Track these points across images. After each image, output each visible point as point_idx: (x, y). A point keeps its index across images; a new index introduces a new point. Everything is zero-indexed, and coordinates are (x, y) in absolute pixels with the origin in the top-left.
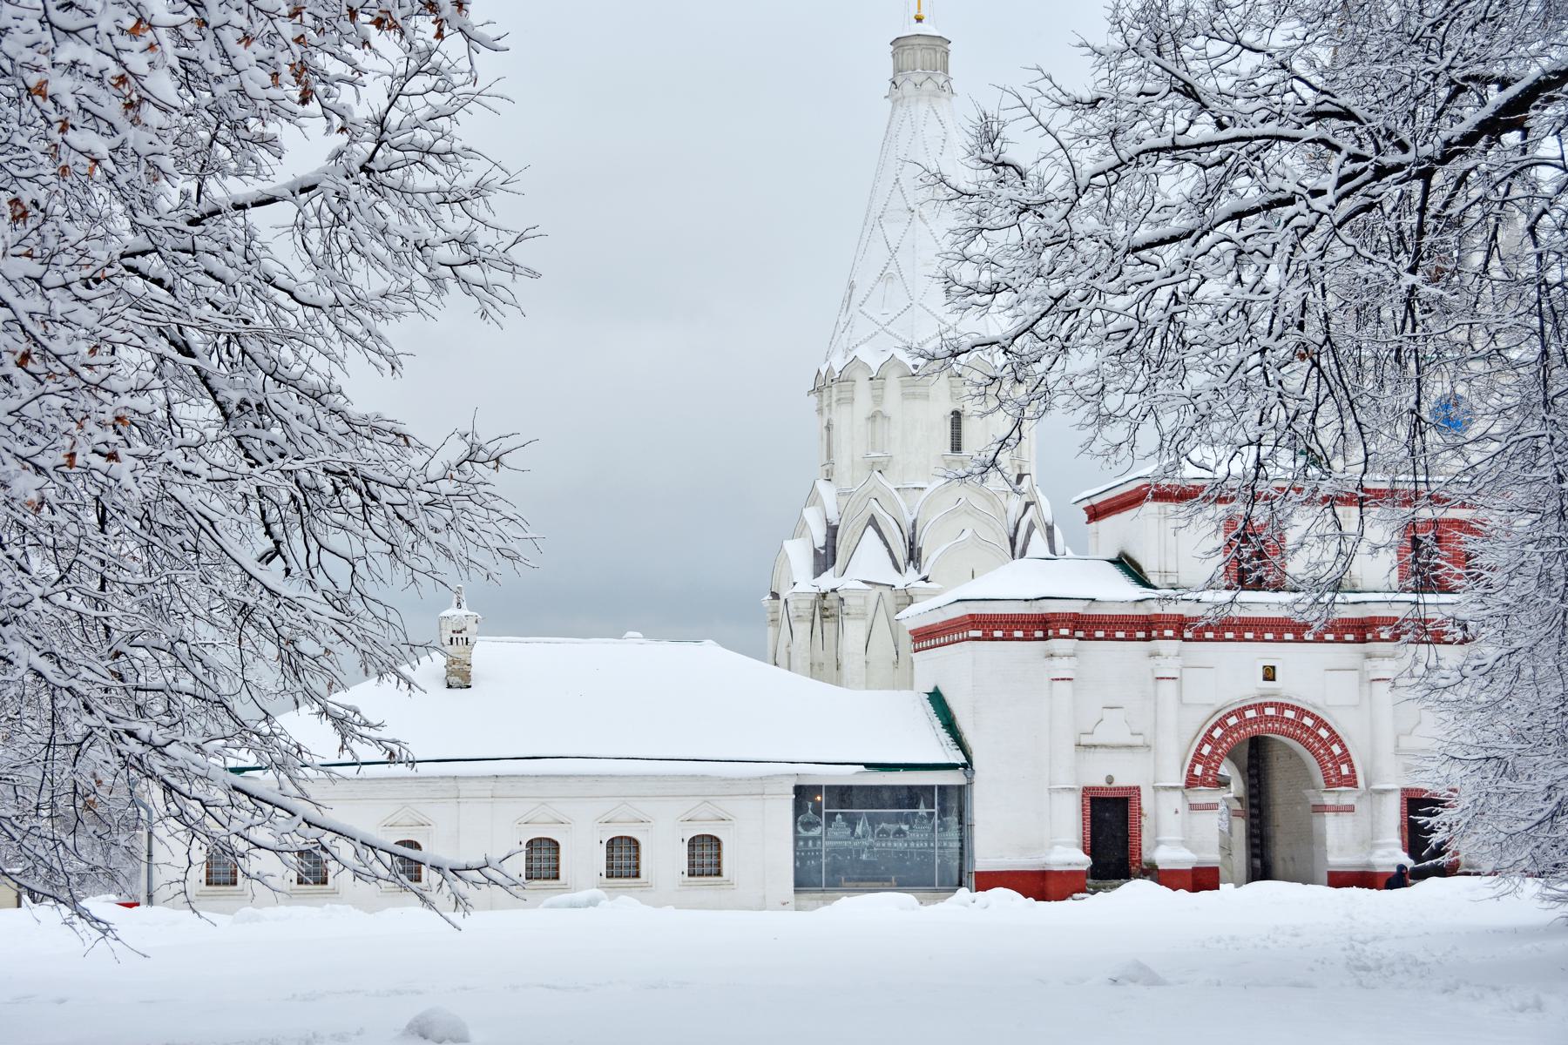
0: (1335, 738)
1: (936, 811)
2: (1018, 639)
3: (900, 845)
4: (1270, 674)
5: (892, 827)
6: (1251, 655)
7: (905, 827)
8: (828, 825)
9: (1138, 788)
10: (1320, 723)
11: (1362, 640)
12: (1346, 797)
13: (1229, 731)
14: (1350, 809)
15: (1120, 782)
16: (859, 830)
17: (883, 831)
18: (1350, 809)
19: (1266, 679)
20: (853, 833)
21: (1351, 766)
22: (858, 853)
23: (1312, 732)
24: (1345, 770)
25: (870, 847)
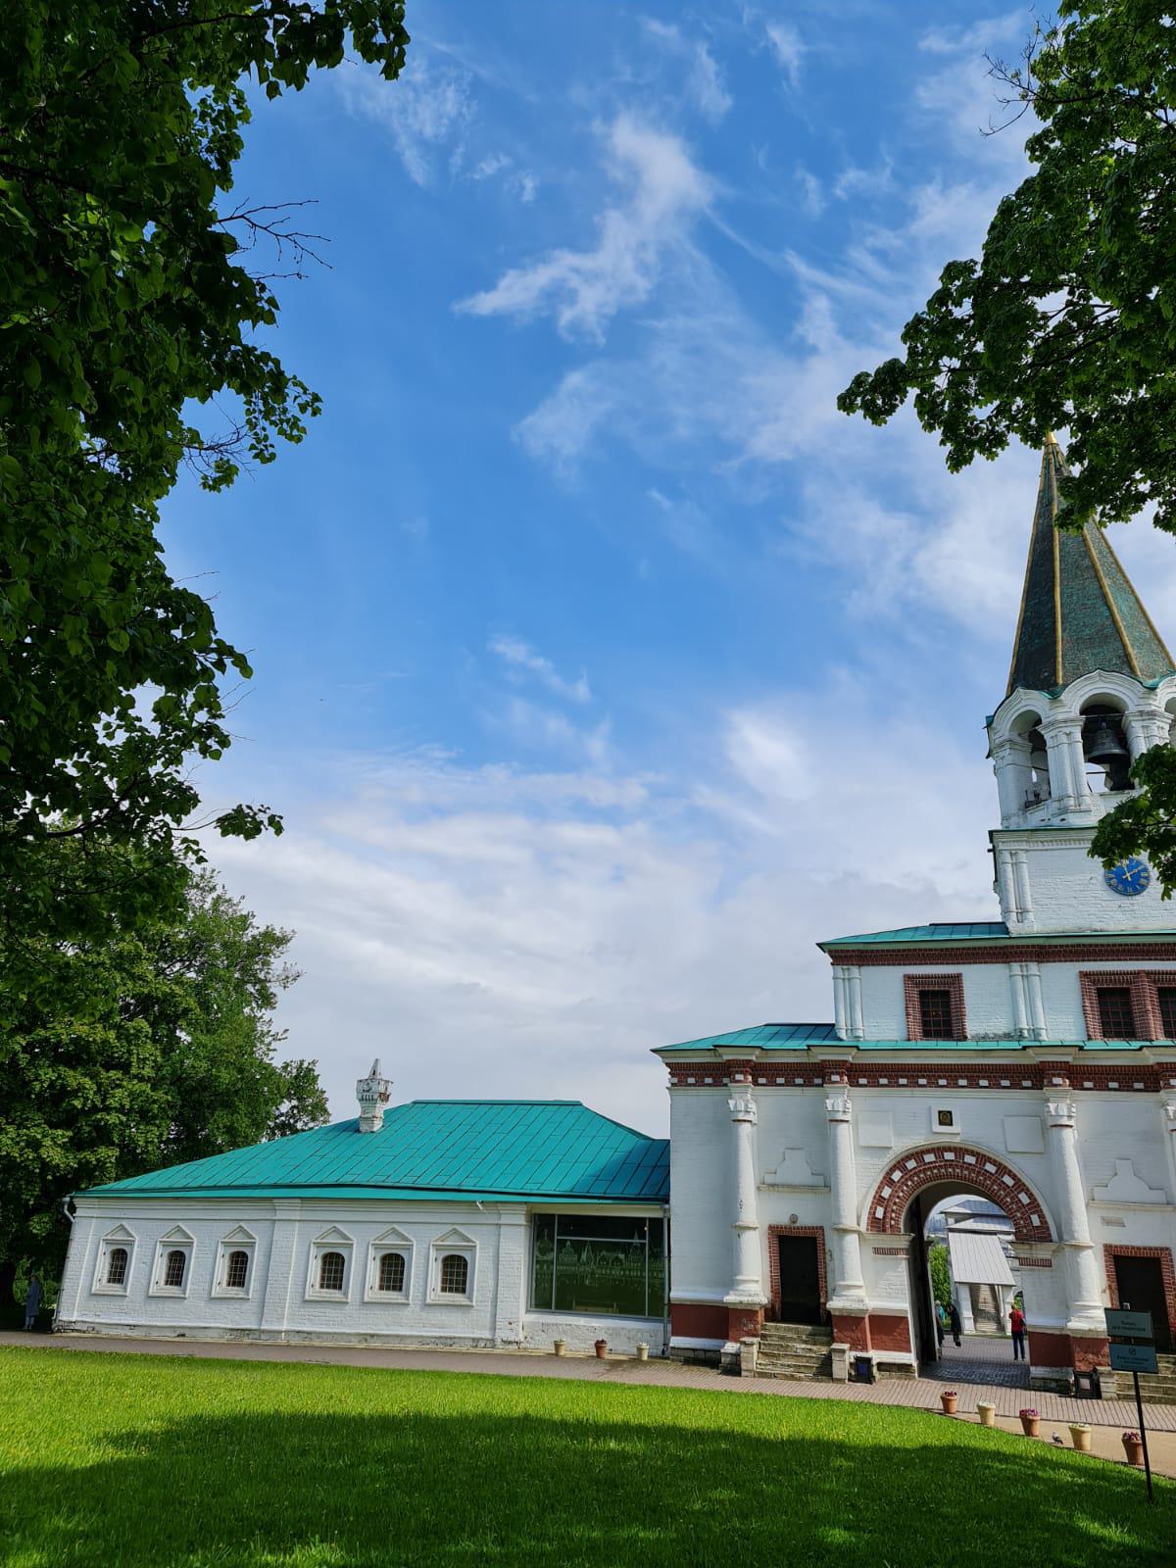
0: (1020, 1186)
2: (709, 1085)
3: (617, 1272)
4: (946, 1118)
7: (622, 1256)
8: (559, 1251)
9: (822, 1228)
10: (1003, 1170)
11: (1038, 1086)
14: (1047, 1264)
15: (807, 1219)
16: (584, 1257)
17: (603, 1258)
18: (1047, 1264)
19: (941, 1123)
20: (579, 1259)
21: (1042, 1217)
22: (583, 1278)
23: (996, 1178)
24: (1036, 1220)
25: (593, 1273)
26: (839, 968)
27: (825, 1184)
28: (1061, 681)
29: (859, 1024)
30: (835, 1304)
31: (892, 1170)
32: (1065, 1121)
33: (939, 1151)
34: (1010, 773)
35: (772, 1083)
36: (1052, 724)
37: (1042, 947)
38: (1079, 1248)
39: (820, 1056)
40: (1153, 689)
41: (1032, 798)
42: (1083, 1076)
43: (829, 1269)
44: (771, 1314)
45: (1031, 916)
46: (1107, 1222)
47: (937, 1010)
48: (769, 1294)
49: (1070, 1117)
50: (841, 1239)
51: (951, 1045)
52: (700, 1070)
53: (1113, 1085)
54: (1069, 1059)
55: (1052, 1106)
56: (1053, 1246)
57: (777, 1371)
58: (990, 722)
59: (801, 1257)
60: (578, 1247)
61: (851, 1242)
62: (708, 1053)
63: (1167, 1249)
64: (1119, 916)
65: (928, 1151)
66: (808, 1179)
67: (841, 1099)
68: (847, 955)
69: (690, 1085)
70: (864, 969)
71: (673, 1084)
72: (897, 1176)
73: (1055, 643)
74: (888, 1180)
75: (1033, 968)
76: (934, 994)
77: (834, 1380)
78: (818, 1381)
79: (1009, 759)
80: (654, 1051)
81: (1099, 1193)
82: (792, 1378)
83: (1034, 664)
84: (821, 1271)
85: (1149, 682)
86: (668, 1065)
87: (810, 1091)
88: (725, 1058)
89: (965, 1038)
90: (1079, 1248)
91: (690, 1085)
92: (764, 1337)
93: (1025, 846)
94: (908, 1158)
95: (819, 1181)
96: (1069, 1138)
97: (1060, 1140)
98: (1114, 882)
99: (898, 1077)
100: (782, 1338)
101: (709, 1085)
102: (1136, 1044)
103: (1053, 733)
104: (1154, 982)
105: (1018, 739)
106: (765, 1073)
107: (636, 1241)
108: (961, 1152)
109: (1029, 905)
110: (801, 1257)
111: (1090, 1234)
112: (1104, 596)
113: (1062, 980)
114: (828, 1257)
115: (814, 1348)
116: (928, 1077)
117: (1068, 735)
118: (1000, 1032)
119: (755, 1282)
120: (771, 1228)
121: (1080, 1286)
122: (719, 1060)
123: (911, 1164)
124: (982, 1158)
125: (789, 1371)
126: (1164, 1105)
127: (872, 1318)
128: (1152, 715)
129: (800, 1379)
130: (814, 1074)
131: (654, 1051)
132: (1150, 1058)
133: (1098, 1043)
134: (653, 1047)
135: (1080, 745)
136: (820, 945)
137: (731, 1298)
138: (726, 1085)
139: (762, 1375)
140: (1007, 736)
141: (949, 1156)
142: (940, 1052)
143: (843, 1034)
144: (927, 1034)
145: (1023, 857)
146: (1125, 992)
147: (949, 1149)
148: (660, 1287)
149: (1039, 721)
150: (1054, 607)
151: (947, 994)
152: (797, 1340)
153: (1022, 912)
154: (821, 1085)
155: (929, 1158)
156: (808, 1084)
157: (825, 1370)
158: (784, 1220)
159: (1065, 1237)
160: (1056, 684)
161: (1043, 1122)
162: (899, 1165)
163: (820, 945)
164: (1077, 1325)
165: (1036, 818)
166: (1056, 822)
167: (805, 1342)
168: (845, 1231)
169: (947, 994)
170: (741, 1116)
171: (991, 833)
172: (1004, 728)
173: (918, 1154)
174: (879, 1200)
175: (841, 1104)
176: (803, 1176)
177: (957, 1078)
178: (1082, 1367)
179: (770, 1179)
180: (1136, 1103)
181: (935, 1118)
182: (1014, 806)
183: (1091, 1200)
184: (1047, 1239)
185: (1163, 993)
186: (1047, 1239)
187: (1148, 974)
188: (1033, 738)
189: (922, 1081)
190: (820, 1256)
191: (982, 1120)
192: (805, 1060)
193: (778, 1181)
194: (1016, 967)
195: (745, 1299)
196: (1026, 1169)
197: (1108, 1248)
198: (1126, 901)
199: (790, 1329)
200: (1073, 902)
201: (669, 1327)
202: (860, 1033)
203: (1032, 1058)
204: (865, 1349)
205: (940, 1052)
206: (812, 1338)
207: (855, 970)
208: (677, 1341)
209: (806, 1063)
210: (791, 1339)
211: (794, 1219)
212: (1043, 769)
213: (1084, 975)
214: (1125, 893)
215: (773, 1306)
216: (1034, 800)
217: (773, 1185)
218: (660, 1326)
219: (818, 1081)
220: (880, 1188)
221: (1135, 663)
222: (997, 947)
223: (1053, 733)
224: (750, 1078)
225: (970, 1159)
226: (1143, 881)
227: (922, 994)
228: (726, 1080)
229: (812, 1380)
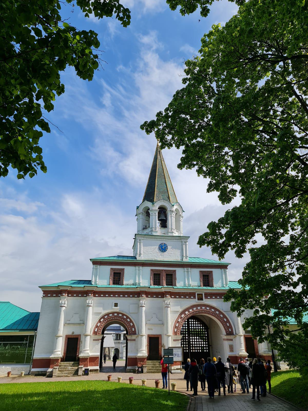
0: (131, 321)
1: (28, 342)
2: (54, 296)
3: (17, 352)
5: (16, 347)
6: (113, 300)
7: (19, 347)
10: (128, 317)
11: (138, 297)
12: (134, 337)
13: (126, 320)
14: (134, 340)
15: (76, 333)
16: (7, 348)
18: (134, 340)
19: (115, 306)
20: (5, 349)
21: (135, 329)
22: (5, 354)
24: (133, 330)
25: (9, 352)
26: (94, 266)
27: (83, 323)
28: (155, 201)
29: (98, 281)
30: (81, 355)
31: (101, 319)
32: (143, 305)
33: (113, 313)
34: (141, 220)
35: (72, 296)
36: (152, 210)
37: (143, 263)
38: (142, 336)
39: (86, 289)
40: (173, 205)
41: (145, 227)
42: (150, 294)
43: (81, 346)
44: (63, 360)
45: (142, 255)
46: (149, 329)
47: (117, 277)
48: (63, 354)
49: (145, 304)
50: (85, 338)
51: (120, 286)
52: (53, 293)
53: (155, 296)
54: (146, 290)
55: (141, 301)
56: (136, 336)
57: (63, 375)
58: (138, 208)
59: (73, 344)
60: (5, 345)
61: (88, 338)
62: (55, 288)
63: (160, 335)
64: (160, 256)
65: (111, 313)
66: (79, 322)
67: (91, 300)
68: (96, 262)
69: (49, 296)
70: (101, 266)
71: (44, 296)
72: (102, 320)
73: (154, 192)
74: (100, 321)
75: (141, 267)
76: (117, 273)
77: (78, 376)
78: (74, 376)
79: (141, 217)
80: (39, 287)
81: (148, 322)
82: (67, 376)
83: (149, 195)
84: (78, 347)
85: (172, 204)
86: (43, 291)
87: (82, 298)
88: (61, 289)
89: (123, 285)
90: (142, 336)
91: (49, 296)
92: (60, 366)
93: (143, 238)
94: (105, 315)
95: (82, 322)
96: (144, 309)
97: (142, 310)
98: (161, 248)
99: (106, 294)
100: (65, 366)
101: (54, 296)
102: (160, 287)
103: (152, 212)
104: (166, 272)
105: (144, 213)
106: (71, 293)
107: (24, 342)
108: (118, 313)
109: (142, 253)
110: (73, 344)
111: (145, 332)
112: (166, 183)
113: (147, 270)
114: (81, 343)
115: (74, 368)
116: (113, 294)
117: (155, 213)
118: (131, 283)
119: (59, 351)
120: (66, 336)
121: (141, 345)
122: (58, 290)
123: (106, 317)
124: (123, 315)
125: (66, 375)
126: (164, 301)
127: (90, 358)
128: (173, 211)
129: (69, 376)
130: (84, 293)
131: (39, 287)
132: (163, 290)
133: (152, 286)
134: (40, 286)
135: (157, 216)
136: (90, 259)
137: (52, 356)
138: (60, 296)
139: (58, 376)
140: (141, 212)
141: (116, 314)
142: (117, 288)
143: (93, 283)
144: (114, 283)
145: (142, 241)
146: (159, 274)
147: (116, 313)
148: (30, 355)
149: (149, 209)
150: (155, 183)
151: (120, 273)
152: (69, 366)
153: (140, 254)
154: (86, 297)
155: (111, 315)
156: (82, 296)
157: (76, 373)
158: (70, 333)
159: (140, 333)
160: (154, 201)
161: (139, 305)
162: (103, 317)
163: (90, 259)
164: (140, 355)
165: (146, 232)
166: (150, 233)
167: (71, 366)
168: (87, 335)
169: (120, 273)
170: (63, 305)
171: (136, 234)
172: (141, 209)
173: (108, 314)
174: (97, 326)
175: (91, 301)
176: (78, 321)
177: (120, 295)
178: (139, 365)
179: (68, 322)
180: (159, 300)
181: (114, 305)
182: (141, 228)
183: (146, 324)
184: (135, 334)
185: (167, 275)
186: (135, 334)
187: (165, 270)
188: (147, 213)
189: (112, 296)
190: (79, 343)
191: (124, 305)
192: (83, 290)
193: (70, 323)
194: (137, 267)
195: (56, 356)
196: (133, 317)
197: (148, 335)
198: (162, 253)
199: (67, 363)
200: (151, 253)
201: (32, 366)
202: (98, 283)
203: (138, 290)
204: (87, 366)
205: (117, 288)
206: (73, 365)
207: (99, 266)
208: (34, 370)
209: (83, 291)
210: (68, 366)
211: (73, 333)
212: (148, 221)
213: (152, 270)
214: (162, 251)
215: (63, 357)
216: (145, 228)
217: (69, 324)
218: (29, 366)
219: (85, 295)
220: (97, 323)
221: (170, 199)
222: (134, 262)
223: (152, 212)
224: (67, 294)
225: (120, 315)
226: (166, 249)
227: (114, 273)
228: (59, 295)
229: (72, 376)
